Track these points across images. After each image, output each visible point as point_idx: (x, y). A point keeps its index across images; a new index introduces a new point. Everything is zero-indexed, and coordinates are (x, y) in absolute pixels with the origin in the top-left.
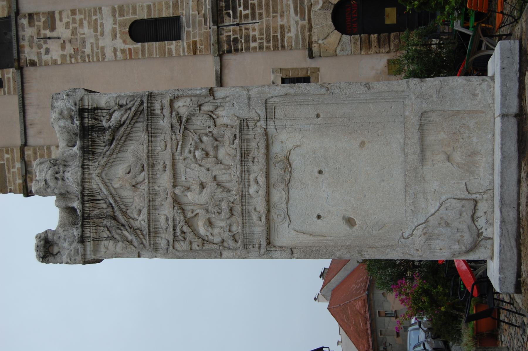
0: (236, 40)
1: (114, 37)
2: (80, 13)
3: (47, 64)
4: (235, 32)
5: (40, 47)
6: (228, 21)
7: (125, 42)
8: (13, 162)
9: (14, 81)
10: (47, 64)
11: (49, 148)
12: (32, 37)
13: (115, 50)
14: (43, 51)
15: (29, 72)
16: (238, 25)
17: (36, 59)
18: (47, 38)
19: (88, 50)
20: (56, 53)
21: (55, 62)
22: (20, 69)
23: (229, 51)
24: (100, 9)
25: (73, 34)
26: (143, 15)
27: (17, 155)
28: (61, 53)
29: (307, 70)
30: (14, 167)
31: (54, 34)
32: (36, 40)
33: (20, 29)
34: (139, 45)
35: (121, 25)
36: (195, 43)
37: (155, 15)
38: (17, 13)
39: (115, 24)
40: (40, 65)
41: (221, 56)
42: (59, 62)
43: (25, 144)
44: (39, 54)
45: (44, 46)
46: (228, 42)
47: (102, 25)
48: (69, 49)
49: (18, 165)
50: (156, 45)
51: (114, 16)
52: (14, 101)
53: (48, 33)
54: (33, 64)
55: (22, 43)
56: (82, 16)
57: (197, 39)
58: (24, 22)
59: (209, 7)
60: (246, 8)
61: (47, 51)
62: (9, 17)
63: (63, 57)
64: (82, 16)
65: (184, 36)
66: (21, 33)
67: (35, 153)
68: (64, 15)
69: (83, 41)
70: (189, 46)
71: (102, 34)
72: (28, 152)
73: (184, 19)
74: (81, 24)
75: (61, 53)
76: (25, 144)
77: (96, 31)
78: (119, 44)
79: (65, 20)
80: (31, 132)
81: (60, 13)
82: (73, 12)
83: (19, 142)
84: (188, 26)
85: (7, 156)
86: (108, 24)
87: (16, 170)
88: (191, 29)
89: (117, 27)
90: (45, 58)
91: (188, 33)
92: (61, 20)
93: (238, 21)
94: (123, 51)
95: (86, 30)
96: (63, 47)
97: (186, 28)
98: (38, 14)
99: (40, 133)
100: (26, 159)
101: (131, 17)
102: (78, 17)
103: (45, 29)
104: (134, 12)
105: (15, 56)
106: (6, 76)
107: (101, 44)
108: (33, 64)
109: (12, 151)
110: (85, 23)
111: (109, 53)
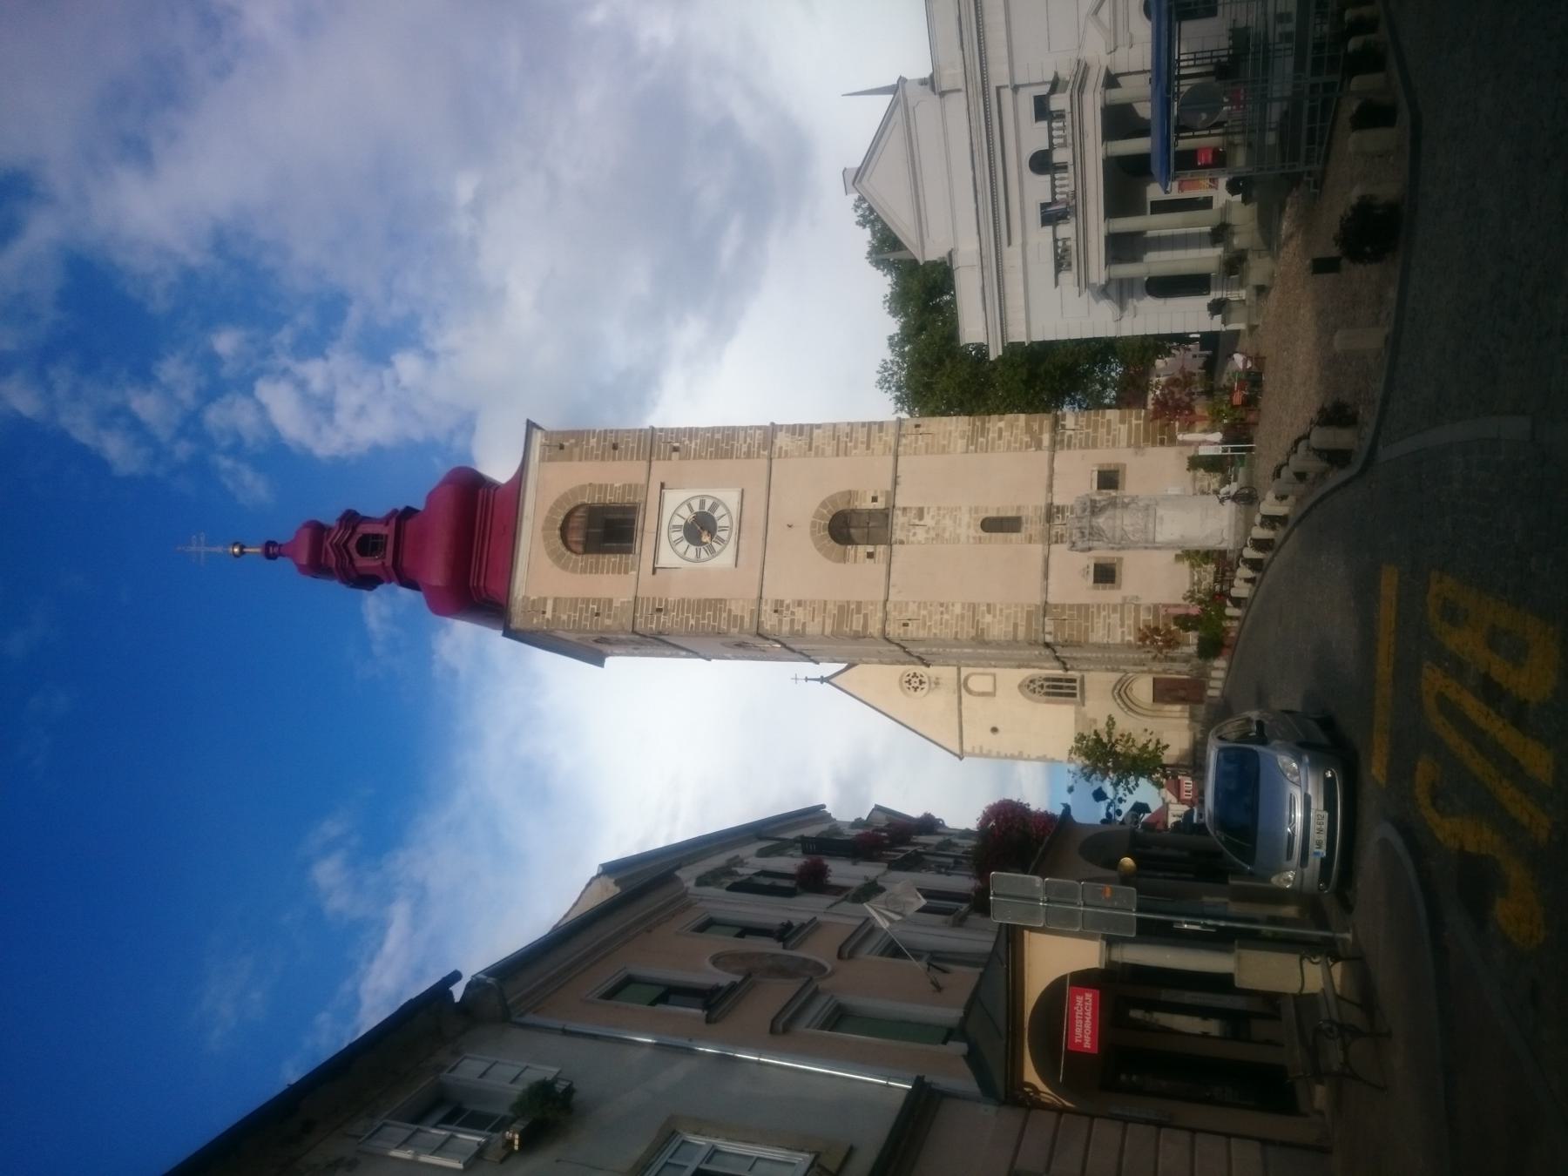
0: (1062, 535)
1: (969, 527)
2: (944, 509)
3: (913, 543)
4: (1062, 530)
5: (909, 531)
6: (1057, 522)
7: (976, 531)
8: (876, 612)
9: (884, 553)
10: (913, 543)
11: (907, 603)
12: (904, 523)
13: (968, 537)
14: (911, 534)
15: (894, 547)
16: (1065, 524)
17: (904, 539)
18: (914, 525)
19: (947, 535)
20: (921, 535)
21: (919, 543)
22: (891, 545)
23: (1056, 542)
24: (960, 508)
25: (936, 524)
26: (993, 514)
27: (880, 607)
28: (925, 536)
29: (1114, 558)
30: (875, 616)
31: (922, 523)
32: (906, 525)
33: (894, 518)
34: (987, 534)
35: (975, 519)
36: (1031, 536)
37: (1002, 514)
38: (894, 506)
39: (971, 517)
40: (908, 543)
41: (1049, 545)
42: (923, 542)
43: (886, 600)
44: (908, 536)
45: (913, 531)
46: (1057, 536)
47: (960, 519)
48: (932, 534)
49: (880, 615)
50: (1000, 535)
51: (971, 514)
52: (883, 567)
53: (917, 522)
54: (902, 542)
55: (894, 527)
56: (946, 512)
57: (1033, 533)
58: (898, 513)
59: (1043, 511)
60: (1072, 513)
61: (915, 534)
62: (887, 509)
63: (927, 539)
64: (946, 512)
65: (1023, 529)
66: (894, 522)
67: (895, 606)
68: (931, 510)
69: (944, 529)
70: (1026, 538)
71: (960, 525)
72: (888, 605)
73: (1024, 519)
74: (944, 516)
75: (925, 536)
76: (886, 600)
77: (955, 522)
78: (972, 532)
79: (931, 514)
80: (892, 591)
81: (929, 508)
82: (939, 509)
83: (882, 598)
84: (1027, 523)
85: (871, 607)
86: (965, 518)
87: (877, 618)
88: (1029, 526)
89: (972, 522)
90: (912, 539)
91: (1026, 528)
92: (928, 513)
93: (1065, 522)
94: (974, 538)
95: (948, 522)
96: (927, 532)
97: (1025, 525)
98: (911, 508)
99: (900, 592)
100: (887, 609)
101: (984, 515)
102: (942, 512)
103: (915, 518)
104: (987, 511)
105: (889, 536)
106: (878, 550)
107: (958, 531)
108: (902, 542)
109: (876, 605)
110: (947, 517)
111: (963, 538)
